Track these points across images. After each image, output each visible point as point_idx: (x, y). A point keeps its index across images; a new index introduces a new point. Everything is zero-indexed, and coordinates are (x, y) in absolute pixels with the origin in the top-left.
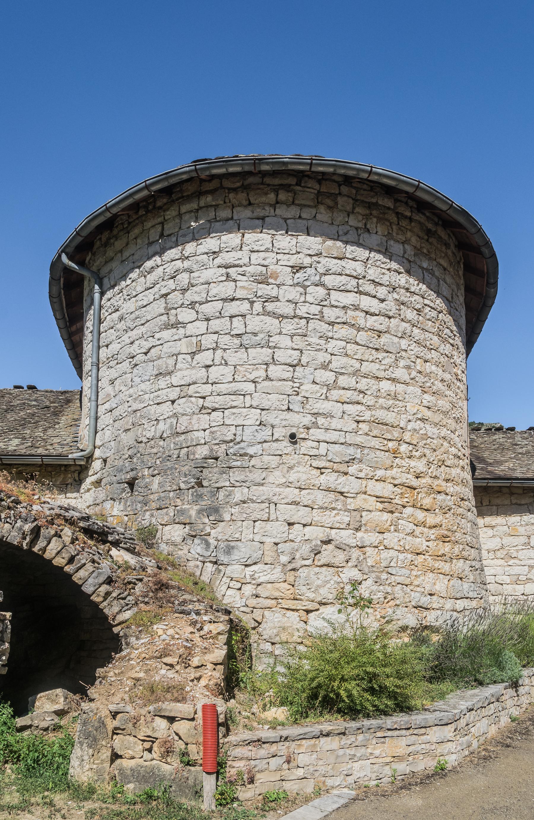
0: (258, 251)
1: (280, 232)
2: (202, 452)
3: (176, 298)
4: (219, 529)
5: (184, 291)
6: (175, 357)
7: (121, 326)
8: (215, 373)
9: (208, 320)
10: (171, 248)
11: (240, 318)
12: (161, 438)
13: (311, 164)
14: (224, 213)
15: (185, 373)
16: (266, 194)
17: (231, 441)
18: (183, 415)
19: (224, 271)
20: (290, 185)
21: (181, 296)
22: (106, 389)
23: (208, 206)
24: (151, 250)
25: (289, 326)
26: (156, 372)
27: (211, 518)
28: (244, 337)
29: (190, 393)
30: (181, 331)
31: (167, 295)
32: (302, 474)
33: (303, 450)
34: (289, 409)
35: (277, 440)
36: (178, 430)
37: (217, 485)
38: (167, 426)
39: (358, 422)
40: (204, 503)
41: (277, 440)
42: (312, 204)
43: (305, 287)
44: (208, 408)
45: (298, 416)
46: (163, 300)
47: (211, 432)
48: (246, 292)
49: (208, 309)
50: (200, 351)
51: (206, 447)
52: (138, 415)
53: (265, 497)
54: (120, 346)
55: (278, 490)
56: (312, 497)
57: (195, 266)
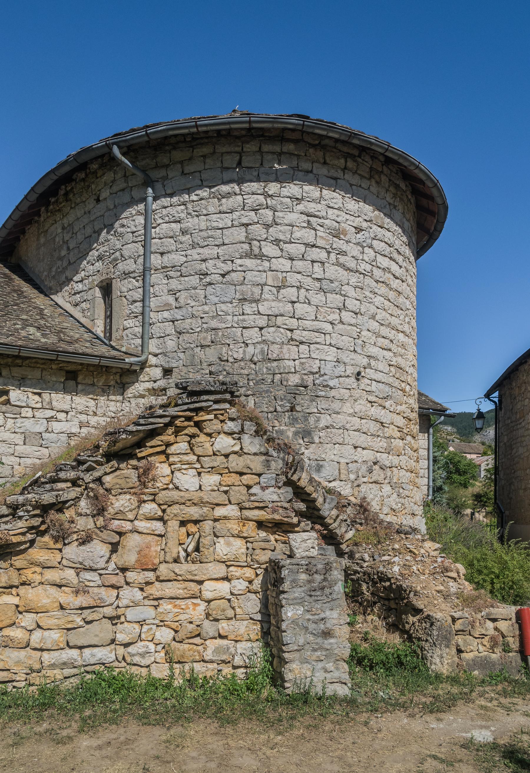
0: (332, 208)
1: (348, 195)
2: (294, 380)
3: (258, 230)
4: (311, 450)
5: (267, 226)
6: (260, 287)
7: (186, 238)
8: (301, 309)
9: (292, 259)
10: (251, 181)
11: (319, 264)
12: (251, 360)
13: (387, 150)
14: (306, 166)
15: (273, 304)
16: (339, 158)
17: (317, 373)
18: (273, 343)
19: (306, 218)
20: (355, 156)
21: (264, 230)
22: (163, 298)
23: (291, 154)
24: (227, 175)
25: (354, 279)
26: (238, 296)
27: (305, 440)
28: (324, 282)
29: (279, 323)
30: (266, 264)
31: (247, 225)
32: (361, 406)
33: (362, 386)
34: (354, 350)
35: (348, 376)
36: (270, 356)
37: (308, 411)
38: (257, 351)
39: (390, 365)
40: (298, 426)
41: (348, 376)
42: (367, 176)
43: (363, 247)
44: (296, 340)
45: (360, 357)
46: (243, 229)
47: (300, 363)
48: (324, 242)
49: (291, 249)
50: (285, 287)
51: (297, 376)
52: (220, 334)
53: (341, 424)
54: (185, 259)
55: (349, 418)
56: (367, 426)
57: (279, 206)
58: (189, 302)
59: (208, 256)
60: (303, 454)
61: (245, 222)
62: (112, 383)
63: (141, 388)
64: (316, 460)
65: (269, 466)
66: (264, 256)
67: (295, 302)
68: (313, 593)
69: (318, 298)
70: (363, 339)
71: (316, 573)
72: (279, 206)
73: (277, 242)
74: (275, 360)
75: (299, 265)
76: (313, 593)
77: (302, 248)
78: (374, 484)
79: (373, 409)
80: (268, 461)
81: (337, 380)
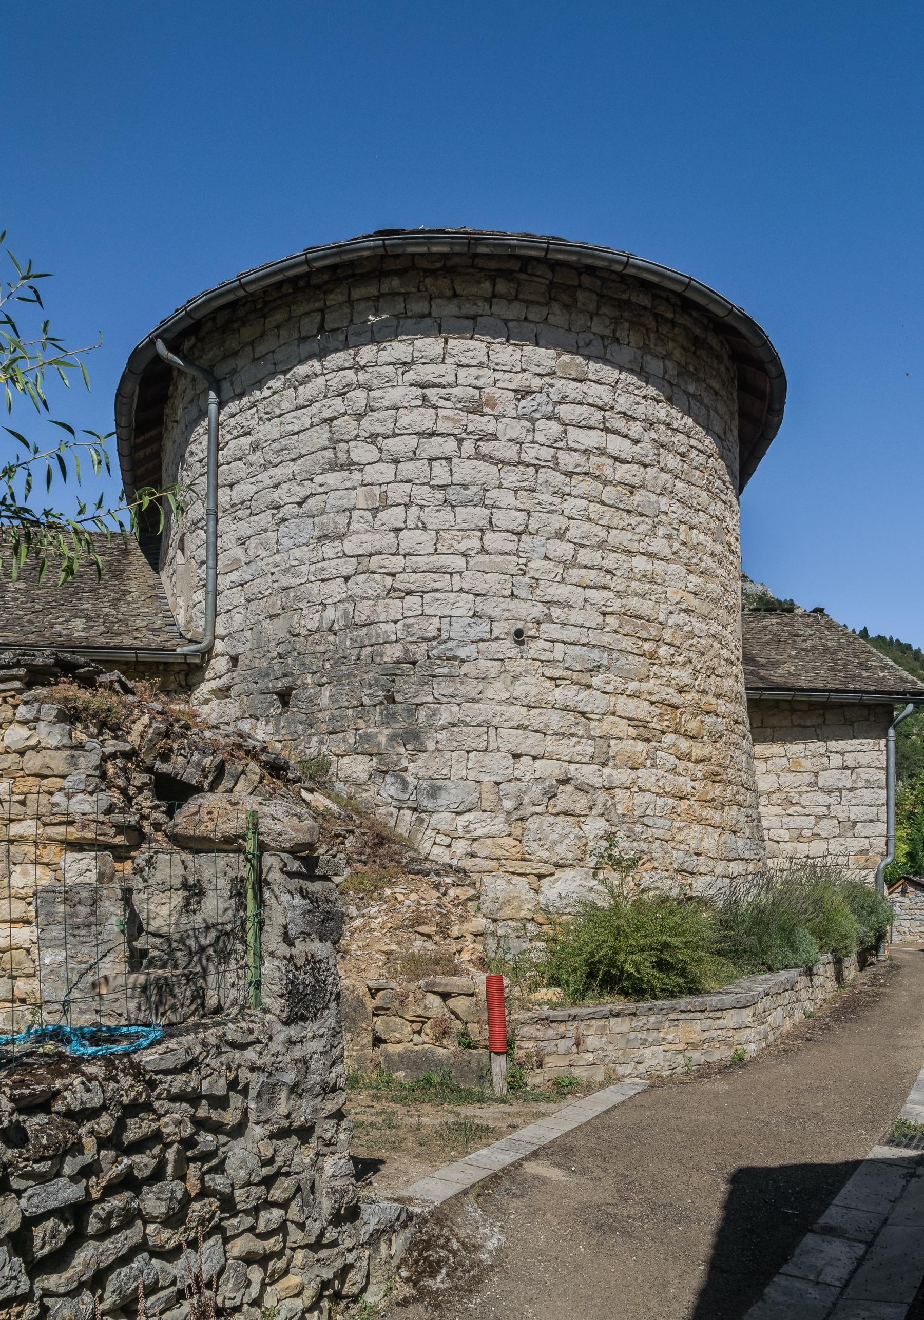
0: (467, 366)
1: (499, 340)
2: (393, 653)
3: (346, 425)
4: (420, 762)
5: (359, 416)
6: (347, 514)
7: (256, 457)
8: (408, 539)
9: (396, 462)
10: (337, 350)
11: (443, 462)
12: (330, 630)
13: (547, 250)
14: (418, 307)
15: (365, 537)
16: (479, 282)
17: (434, 638)
18: (363, 598)
19: (419, 391)
20: (512, 272)
21: (355, 423)
22: (231, 552)
23: (393, 294)
24: (305, 349)
25: (512, 477)
26: (317, 533)
27: (409, 747)
28: (450, 490)
29: (372, 566)
30: (357, 476)
31: (332, 419)
32: (530, 686)
33: (532, 654)
34: (512, 594)
35: (497, 639)
36: (357, 620)
37: (416, 701)
38: (339, 614)
39: (604, 614)
40: (397, 726)
41: (497, 639)
42: (541, 300)
43: (533, 421)
44: (400, 590)
45: (525, 605)
46: (326, 427)
47: (405, 625)
48: (451, 424)
49: (395, 445)
50: (385, 507)
51: (399, 646)
52: (292, 594)
53: (481, 719)
54: (255, 488)
55: (499, 708)
56: (545, 719)
57: (375, 381)
58: (260, 552)
59: (281, 479)
60: (406, 770)
61: (328, 416)
62: (173, 686)
63: (205, 691)
64: (431, 778)
65: (75, 764)
66: (354, 464)
67: (400, 530)
68: (76, 932)
69: (438, 518)
70: (532, 574)
71: (79, 903)
72: (375, 381)
73: (373, 438)
74: (364, 625)
75: (407, 469)
76: (76, 932)
77: (413, 441)
78: (562, 817)
79: (558, 691)
80: (73, 756)
81: (474, 646)
